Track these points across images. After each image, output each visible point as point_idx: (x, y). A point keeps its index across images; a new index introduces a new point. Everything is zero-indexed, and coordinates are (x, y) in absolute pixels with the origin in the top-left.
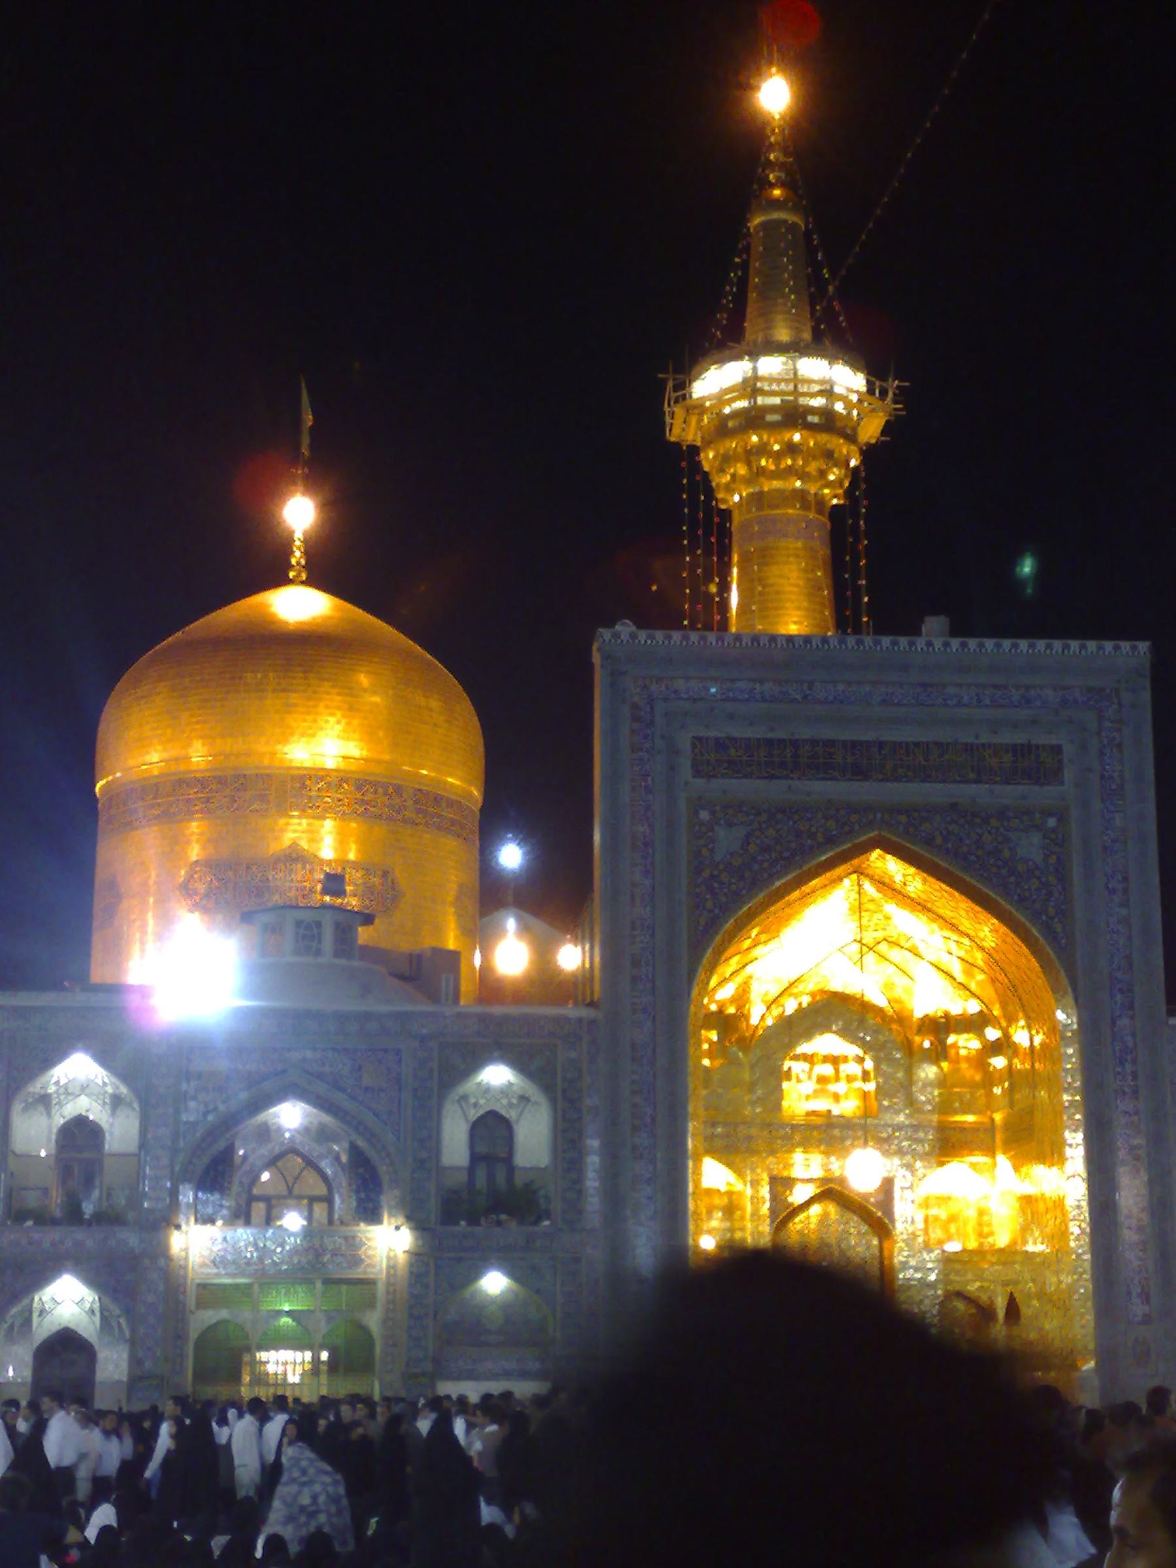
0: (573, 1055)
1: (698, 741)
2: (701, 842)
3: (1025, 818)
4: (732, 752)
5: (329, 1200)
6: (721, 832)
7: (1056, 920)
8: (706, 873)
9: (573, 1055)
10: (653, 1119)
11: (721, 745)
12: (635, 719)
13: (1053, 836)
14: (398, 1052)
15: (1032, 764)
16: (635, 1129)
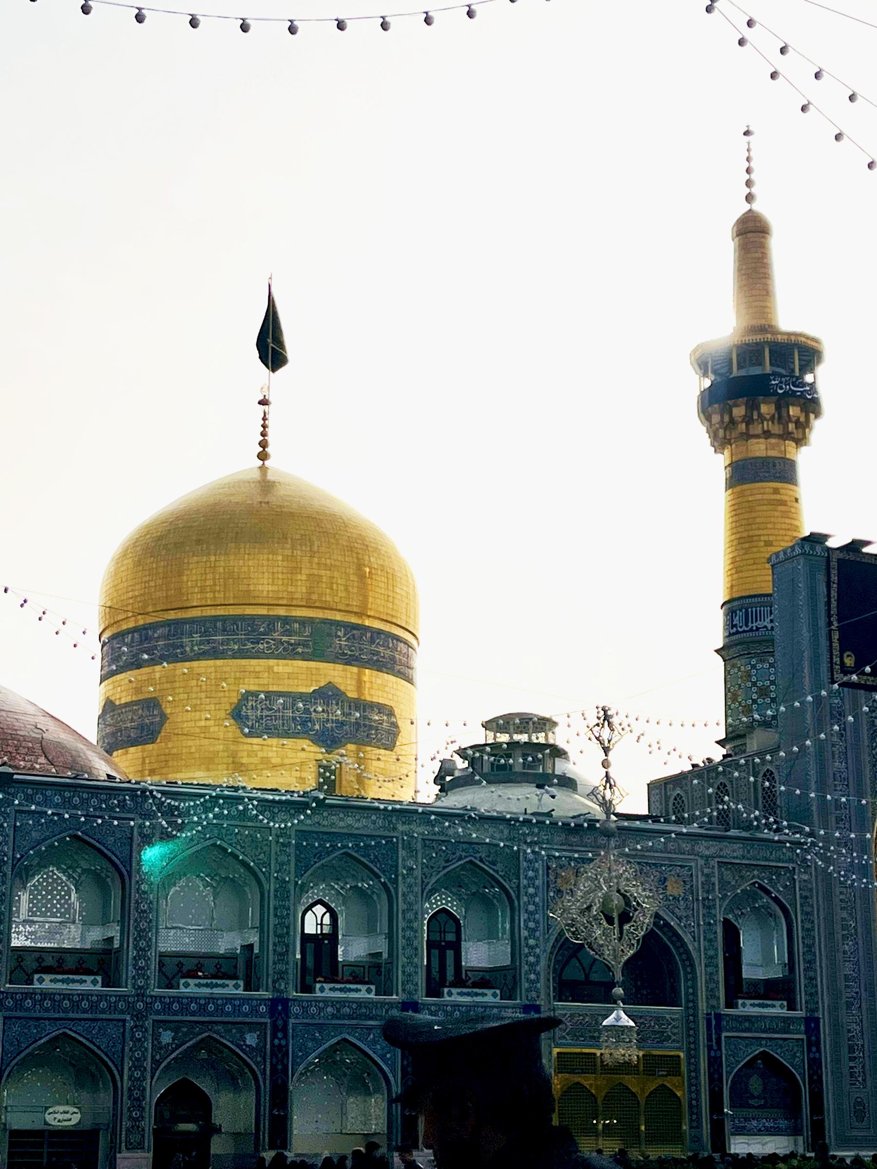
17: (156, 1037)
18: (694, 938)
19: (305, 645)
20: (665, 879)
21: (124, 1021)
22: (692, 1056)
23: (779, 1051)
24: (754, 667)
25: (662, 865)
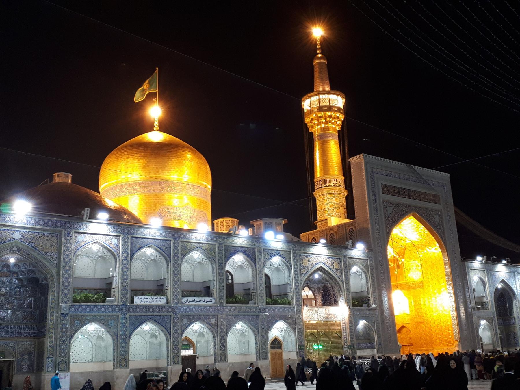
1: (382, 185)
5: (315, 299)
11: (386, 186)
12: (371, 178)
15: (435, 200)
16: (382, 283)
17: (182, 321)
21: (171, 316)
24: (328, 198)
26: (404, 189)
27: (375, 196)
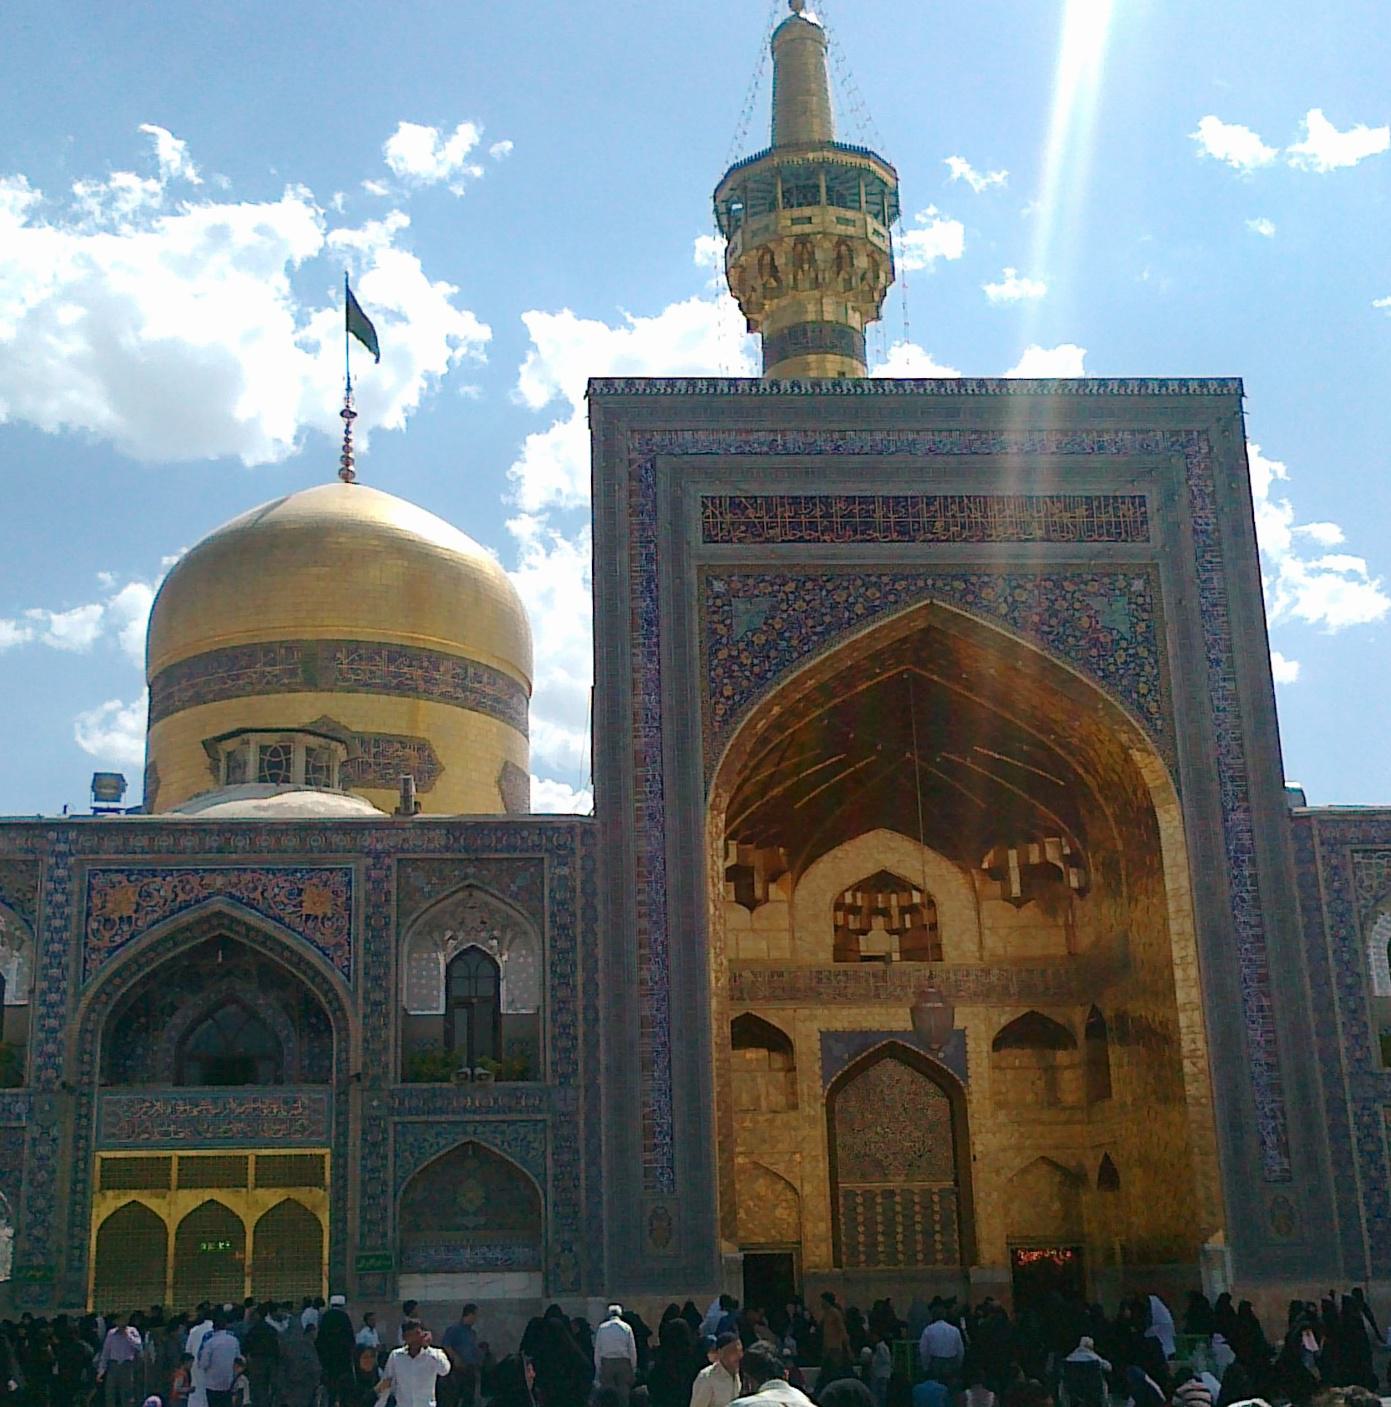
0: (565, 871)
2: (716, 618)
3: (1106, 580)
4: (750, 512)
6: (739, 605)
7: (1149, 698)
8: (723, 654)
9: (565, 871)
10: (665, 947)
11: (735, 504)
13: (1140, 600)
14: (347, 872)
18: (348, 976)
19: (293, 673)
20: (301, 891)
22: (339, 1156)
23: (498, 1142)
25: (296, 871)
26: (864, 500)
27: (650, 559)
